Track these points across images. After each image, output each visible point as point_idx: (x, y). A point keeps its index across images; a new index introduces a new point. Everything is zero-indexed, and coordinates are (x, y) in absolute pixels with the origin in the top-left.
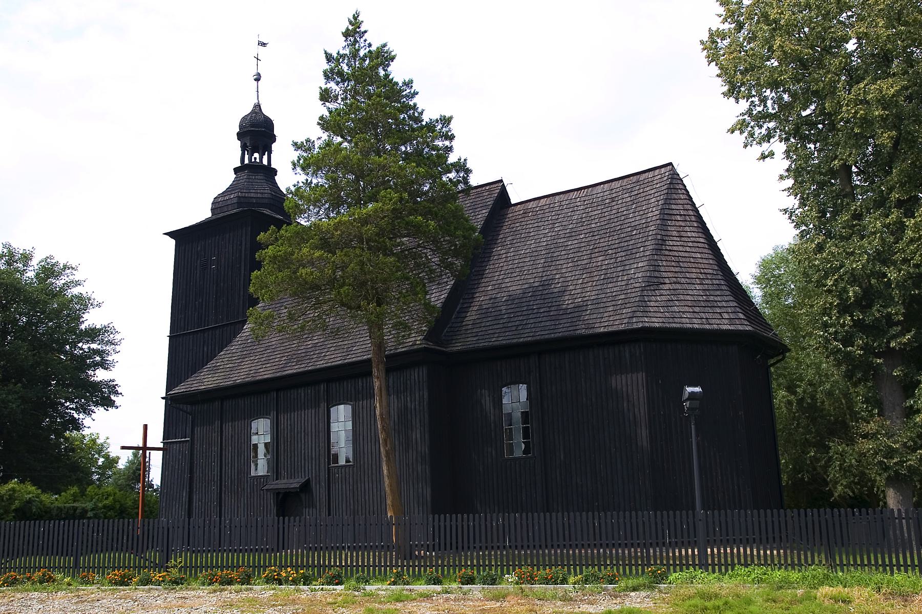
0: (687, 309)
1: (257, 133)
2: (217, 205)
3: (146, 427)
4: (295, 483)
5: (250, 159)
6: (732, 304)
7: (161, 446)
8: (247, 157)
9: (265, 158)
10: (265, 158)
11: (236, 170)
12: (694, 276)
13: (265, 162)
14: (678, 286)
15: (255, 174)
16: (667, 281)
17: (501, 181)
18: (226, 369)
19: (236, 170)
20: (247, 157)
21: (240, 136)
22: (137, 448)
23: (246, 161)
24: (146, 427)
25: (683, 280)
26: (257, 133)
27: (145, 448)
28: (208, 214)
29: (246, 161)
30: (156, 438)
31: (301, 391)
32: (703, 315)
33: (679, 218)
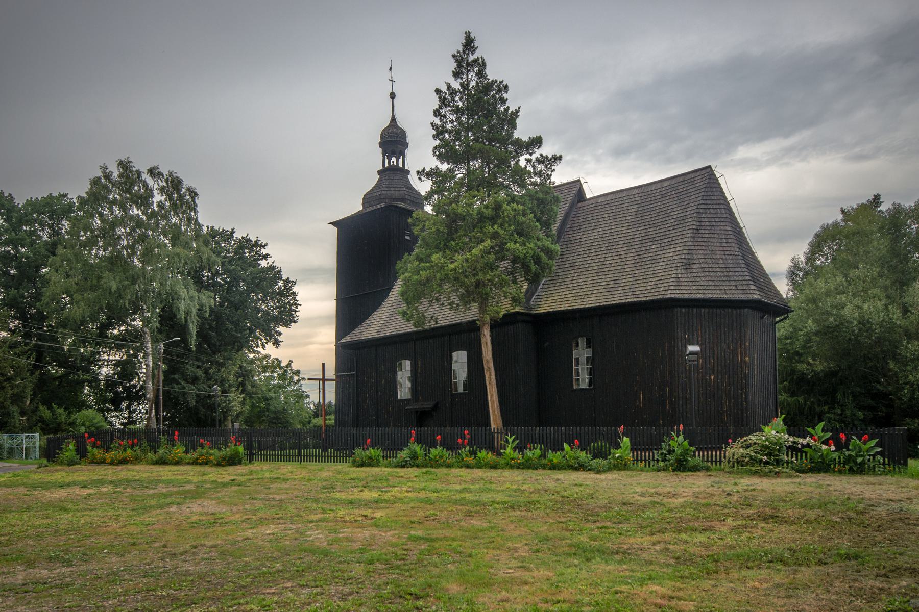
0: (711, 283)
1: (393, 141)
2: (368, 199)
3: (323, 365)
4: (428, 405)
5: (389, 163)
6: (748, 278)
7: (334, 378)
8: (387, 161)
9: (401, 161)
10: (401, 161)
11: (379, 172)
12: (718, 257)
13: (401, 165)
14: (706, 265)
15: (393, 175)
16: (696, 261)
17: (579, 181)
18: (386, 321)
19: (379, 172)
20: (387, 161)
21: (381, 145)
22: (319, 380)
23: (387, 165)
24: (323, 365)
25: (709, 261)
26: (393, 141)
27: (324, 380)
28: (358, 207)
29: (387, 165)
30: (331, 373)
31: (431, 341)
32: (722, 288)
33: (712, 211)
